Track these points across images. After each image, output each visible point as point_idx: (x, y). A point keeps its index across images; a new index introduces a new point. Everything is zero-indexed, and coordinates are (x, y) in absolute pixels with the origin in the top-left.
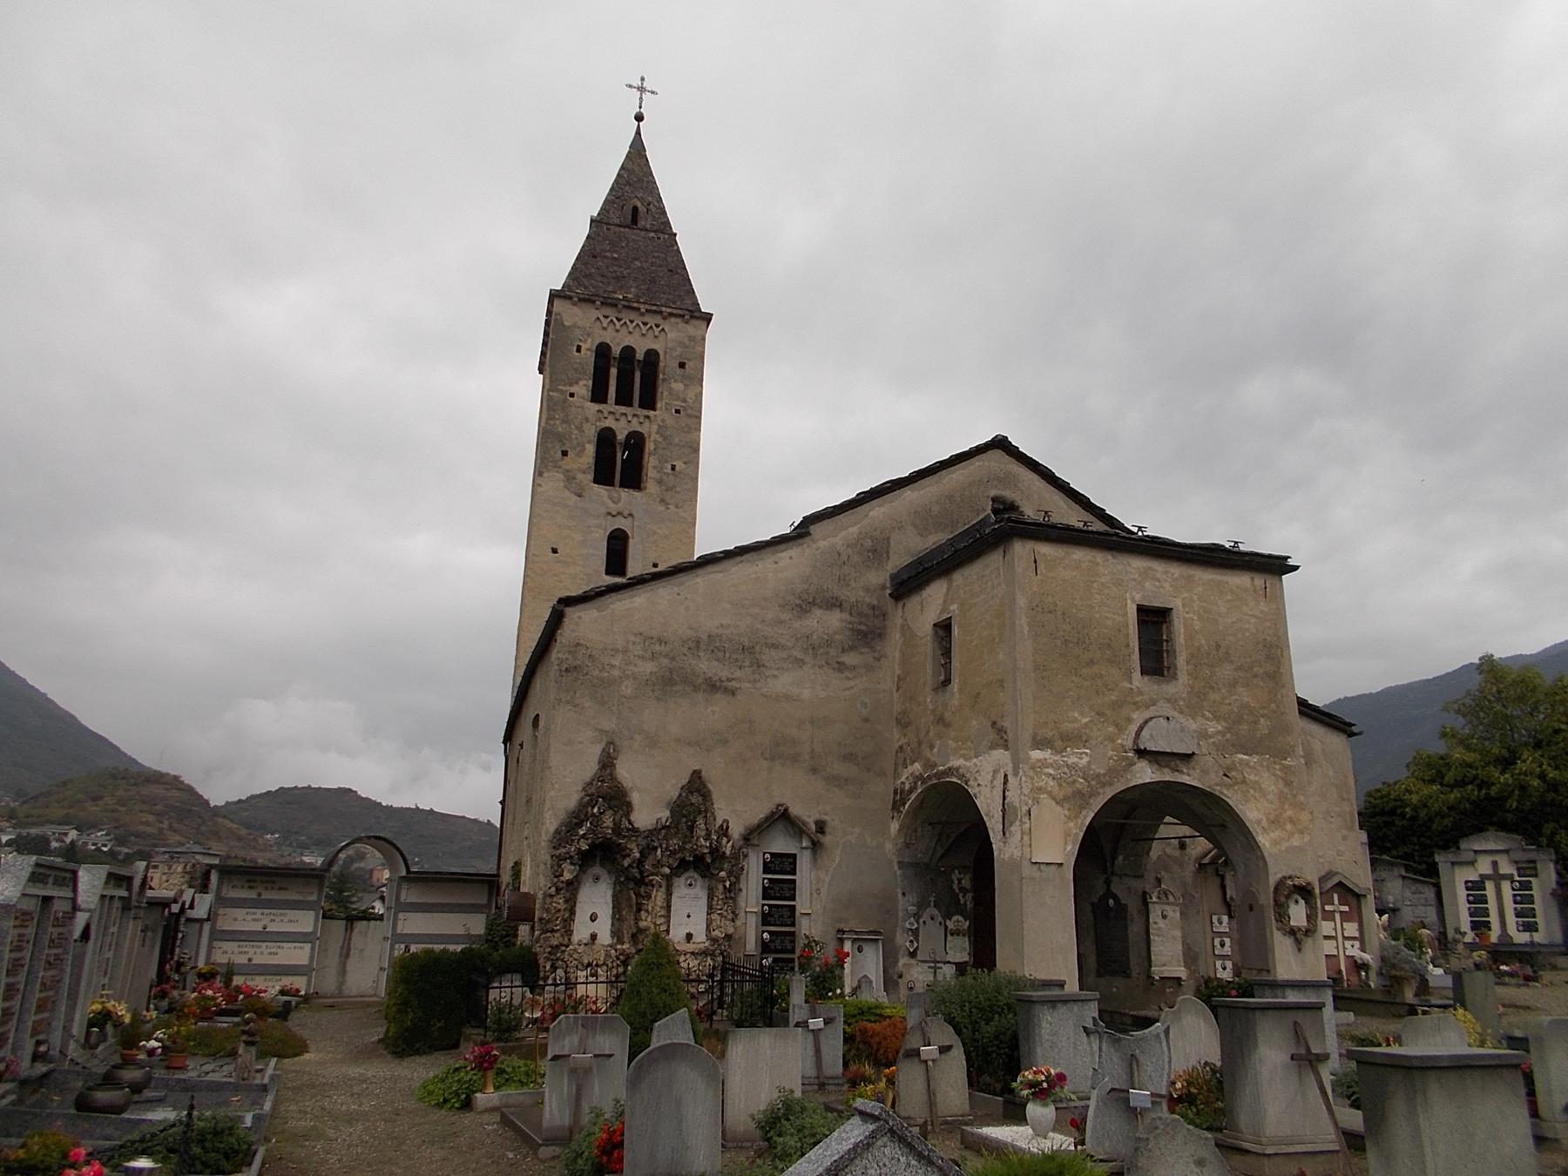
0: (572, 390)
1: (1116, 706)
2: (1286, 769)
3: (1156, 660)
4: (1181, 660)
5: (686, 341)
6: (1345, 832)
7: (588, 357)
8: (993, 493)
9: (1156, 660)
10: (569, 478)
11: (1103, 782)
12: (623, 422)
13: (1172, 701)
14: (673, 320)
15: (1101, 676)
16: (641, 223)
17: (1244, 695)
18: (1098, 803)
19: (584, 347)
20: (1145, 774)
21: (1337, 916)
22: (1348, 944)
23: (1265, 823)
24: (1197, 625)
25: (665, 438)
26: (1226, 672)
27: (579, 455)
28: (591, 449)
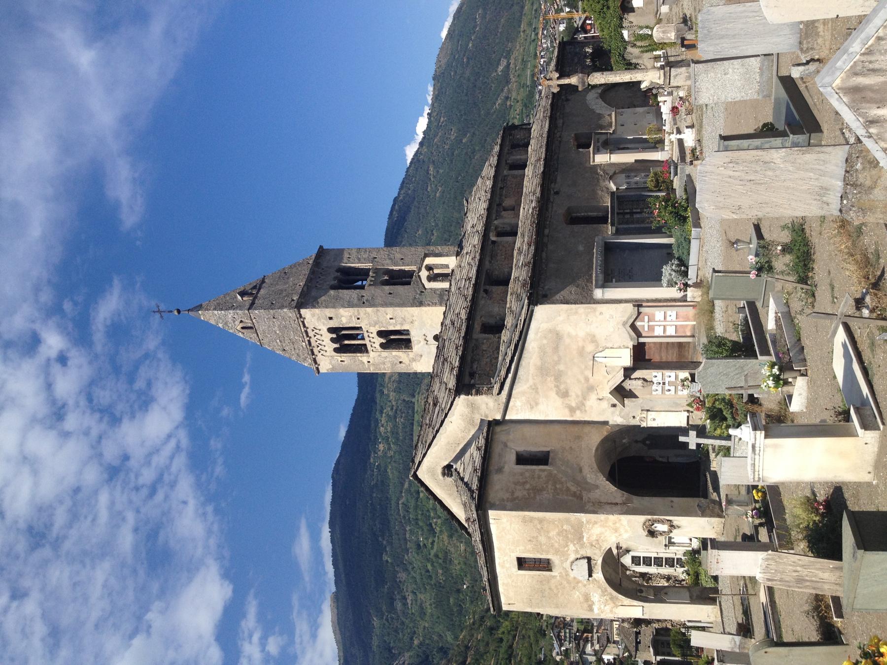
0: (366, 363)
1: (569, 582)
2: (588, 522)
3: (544, 565)
4: (543, 556)
5: (316, 317)
6: (597, 313)
7: (347, 358)
8: (441, 477)
9: (544, 565)
10: (414, 360)
11: (604, 591)
13: (562, 562)
14: (307, 325)
15: (556, 586)
16: (249, 325)
17: (553, 533)
18: (615, 593)
19: (340, 359)
20: (598, 575)
21: (651, 323)
22: (668, 318)
23: (617, 535)
24: (522, 548)
26: (543, 539)
27: (400, 357)
28: (395, 353)
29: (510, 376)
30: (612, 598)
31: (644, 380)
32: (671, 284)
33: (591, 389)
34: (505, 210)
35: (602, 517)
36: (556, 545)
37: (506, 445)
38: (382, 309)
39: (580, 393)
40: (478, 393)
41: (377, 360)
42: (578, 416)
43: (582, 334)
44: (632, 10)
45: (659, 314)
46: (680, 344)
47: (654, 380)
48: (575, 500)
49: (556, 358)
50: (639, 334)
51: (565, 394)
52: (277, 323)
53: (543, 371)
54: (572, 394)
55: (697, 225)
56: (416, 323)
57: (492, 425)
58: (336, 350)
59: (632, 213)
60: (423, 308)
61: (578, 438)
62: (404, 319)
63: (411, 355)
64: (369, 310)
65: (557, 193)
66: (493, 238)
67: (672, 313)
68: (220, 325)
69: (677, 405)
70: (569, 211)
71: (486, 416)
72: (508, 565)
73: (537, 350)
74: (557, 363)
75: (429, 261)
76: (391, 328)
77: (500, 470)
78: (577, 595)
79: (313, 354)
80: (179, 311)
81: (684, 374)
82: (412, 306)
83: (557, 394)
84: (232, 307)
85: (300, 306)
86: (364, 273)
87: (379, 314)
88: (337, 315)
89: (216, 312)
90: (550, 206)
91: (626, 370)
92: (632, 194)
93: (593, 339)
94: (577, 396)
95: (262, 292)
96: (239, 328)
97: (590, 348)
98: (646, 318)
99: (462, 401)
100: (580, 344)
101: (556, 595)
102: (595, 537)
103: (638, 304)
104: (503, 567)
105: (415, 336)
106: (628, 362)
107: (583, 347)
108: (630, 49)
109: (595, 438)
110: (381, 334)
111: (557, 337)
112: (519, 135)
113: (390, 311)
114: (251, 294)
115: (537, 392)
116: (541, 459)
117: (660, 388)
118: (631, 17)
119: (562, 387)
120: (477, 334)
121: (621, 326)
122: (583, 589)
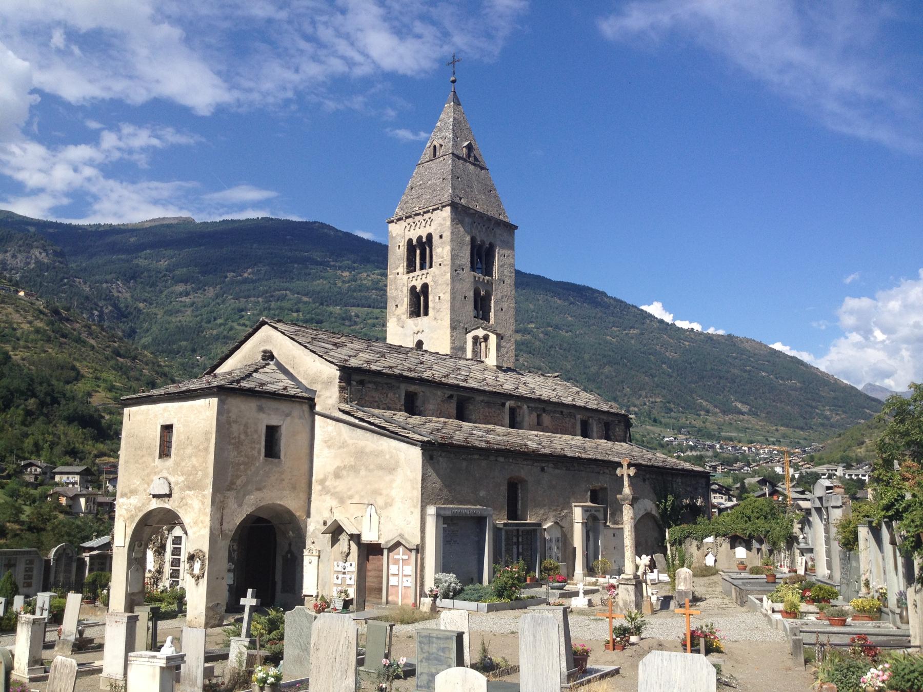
1: (148, 475)
3: (165, 451)
6: (412, 509)
8: (262, 349)
9: (165, 451)
10: (399, 319)
12: (418, 280)
13: (167, 469)
16: (438, 154)
17: (194, 461)
18: (137, 520)
19: (401, 244)
20: (155, 504)
22: (405, 579)
23: (192, 524)
25: (435, 282)
26: (189, 451)
28: (406, 301)
29: (357, 421)
30: (132, 517)
31: (348, 554)
32: (437, 582)
33: (342, 501)
34: (539, 416)
35: (208, 510)
36: (183, 464)
37: (287, 415)
38: (448, 289)
39: (337, 490)
40: (342, 389)
41: (400, 281)
42: (316, 488)
43: (393, 493)
44: (733, 547)
45: (409, 569)
46: (381, 590)
47: (348, 564)
48: (225, 483)
49: (372, 467)
50: (390, 550)
51: (337, 475)
52: (438, 182)
53: (360, 454)
54: (337, 483)
55: (491, 609)
56: (434, 323)
57: (310, 402)
58: (410, 241)
59: (517, 543)
60: (448, 331)
61: (294, 488)
62: (438, 311)
63: (404, 317)
64: (448, 276)
65: (543, 470)
66: (508, 404)
67: (410, 582)
68: (439, 124)
69: (324, 587)
70: (523, 482)
71: (319, 396)
72: (166, 414)
73: (380, 448)
74: (367, 468)
75: (493, 338)
76: (430, 298)
77: (261, 409)
78: (136, 482)
79: (407, 218)
80: (454, 82)
81: (352, 593)
82: (451, 320)
83: (338, 467)
84: (455, 137)
85: (454, 206)
86: (488, 272)
87: (444, 286)
88: (444, 243)
89: (451, 120)
90: (529, 462)
91: (359, 536)
92: (539, 544)
93: (388, 504)
94: (335, 488)
95: (471, 167)
96: (435, 143)
97: (380, 501)
98: (406, 557)
99: (334, 373)
100: (384, 492)
101: (137, 462)
102: (190, 502)
103: (419, 550)
104: (165, 410)
105: (422, 321)
106: (366, 538)
107: (381, 494)
108: (695, 543)
109: (292, 503)
110: (425, 287)
111: (391, 469)
112: (619, 430)
113: (447, 297)
114: (469, 156)
115: (340, 447)
116: (272, 449)
117: (340, 569)
118: (726, 545)
119: (344, 473)
120: (404, 387)
121: (399, 532)
122: (141, 489)
